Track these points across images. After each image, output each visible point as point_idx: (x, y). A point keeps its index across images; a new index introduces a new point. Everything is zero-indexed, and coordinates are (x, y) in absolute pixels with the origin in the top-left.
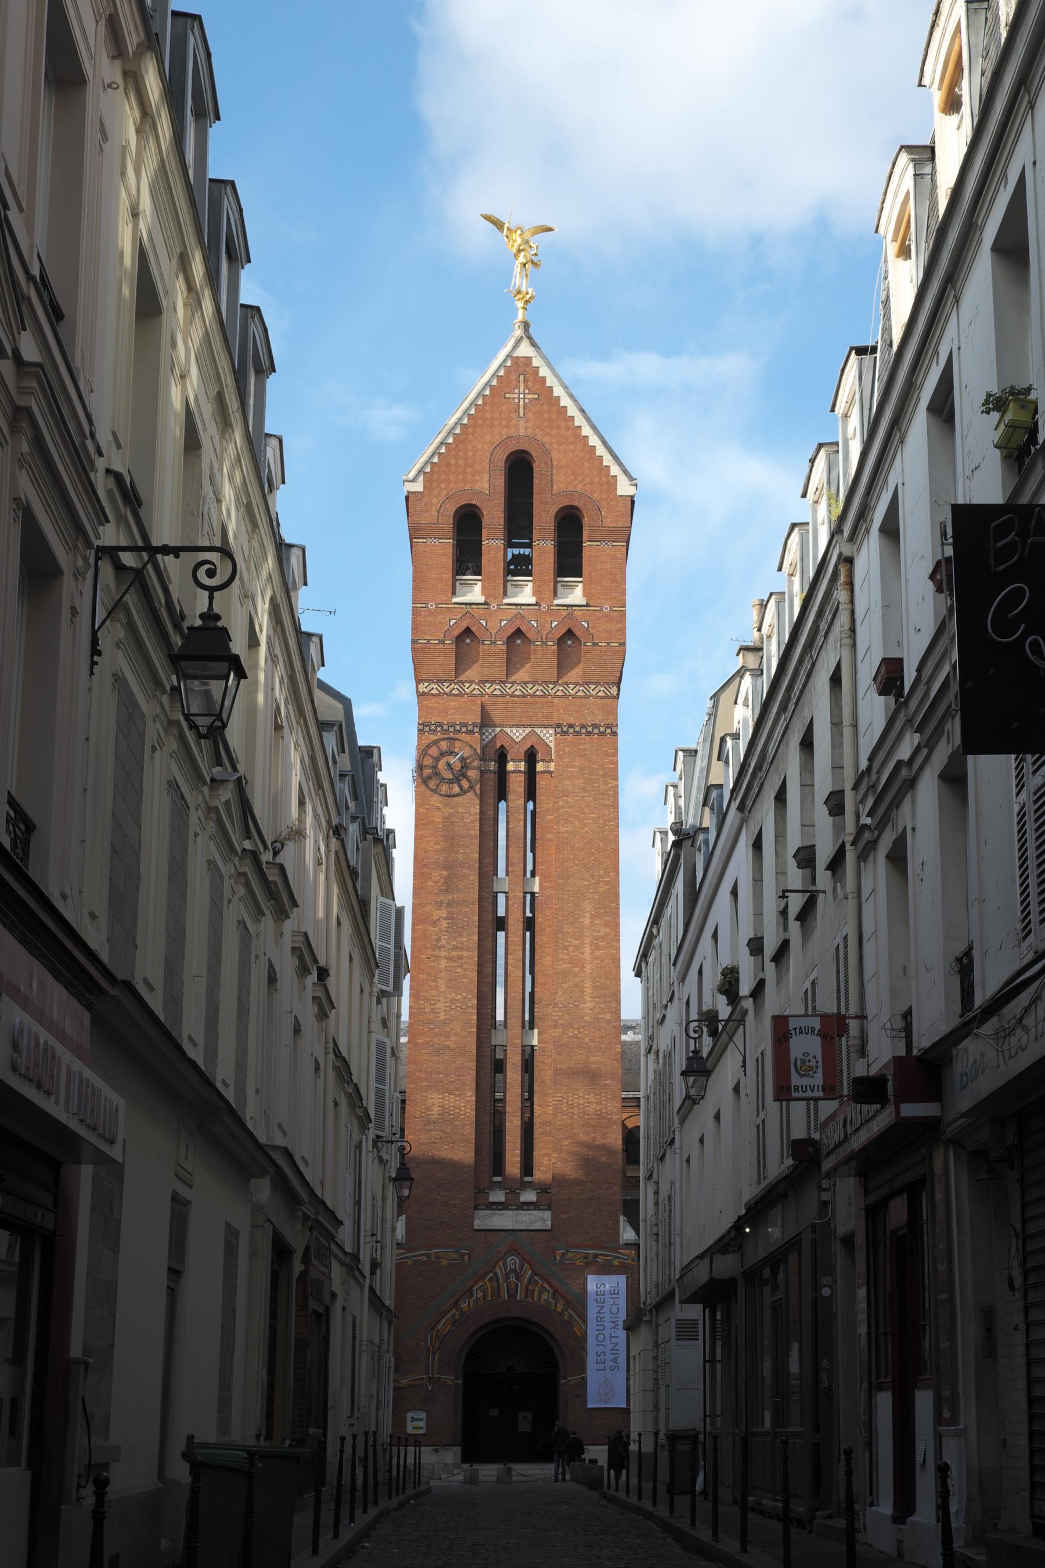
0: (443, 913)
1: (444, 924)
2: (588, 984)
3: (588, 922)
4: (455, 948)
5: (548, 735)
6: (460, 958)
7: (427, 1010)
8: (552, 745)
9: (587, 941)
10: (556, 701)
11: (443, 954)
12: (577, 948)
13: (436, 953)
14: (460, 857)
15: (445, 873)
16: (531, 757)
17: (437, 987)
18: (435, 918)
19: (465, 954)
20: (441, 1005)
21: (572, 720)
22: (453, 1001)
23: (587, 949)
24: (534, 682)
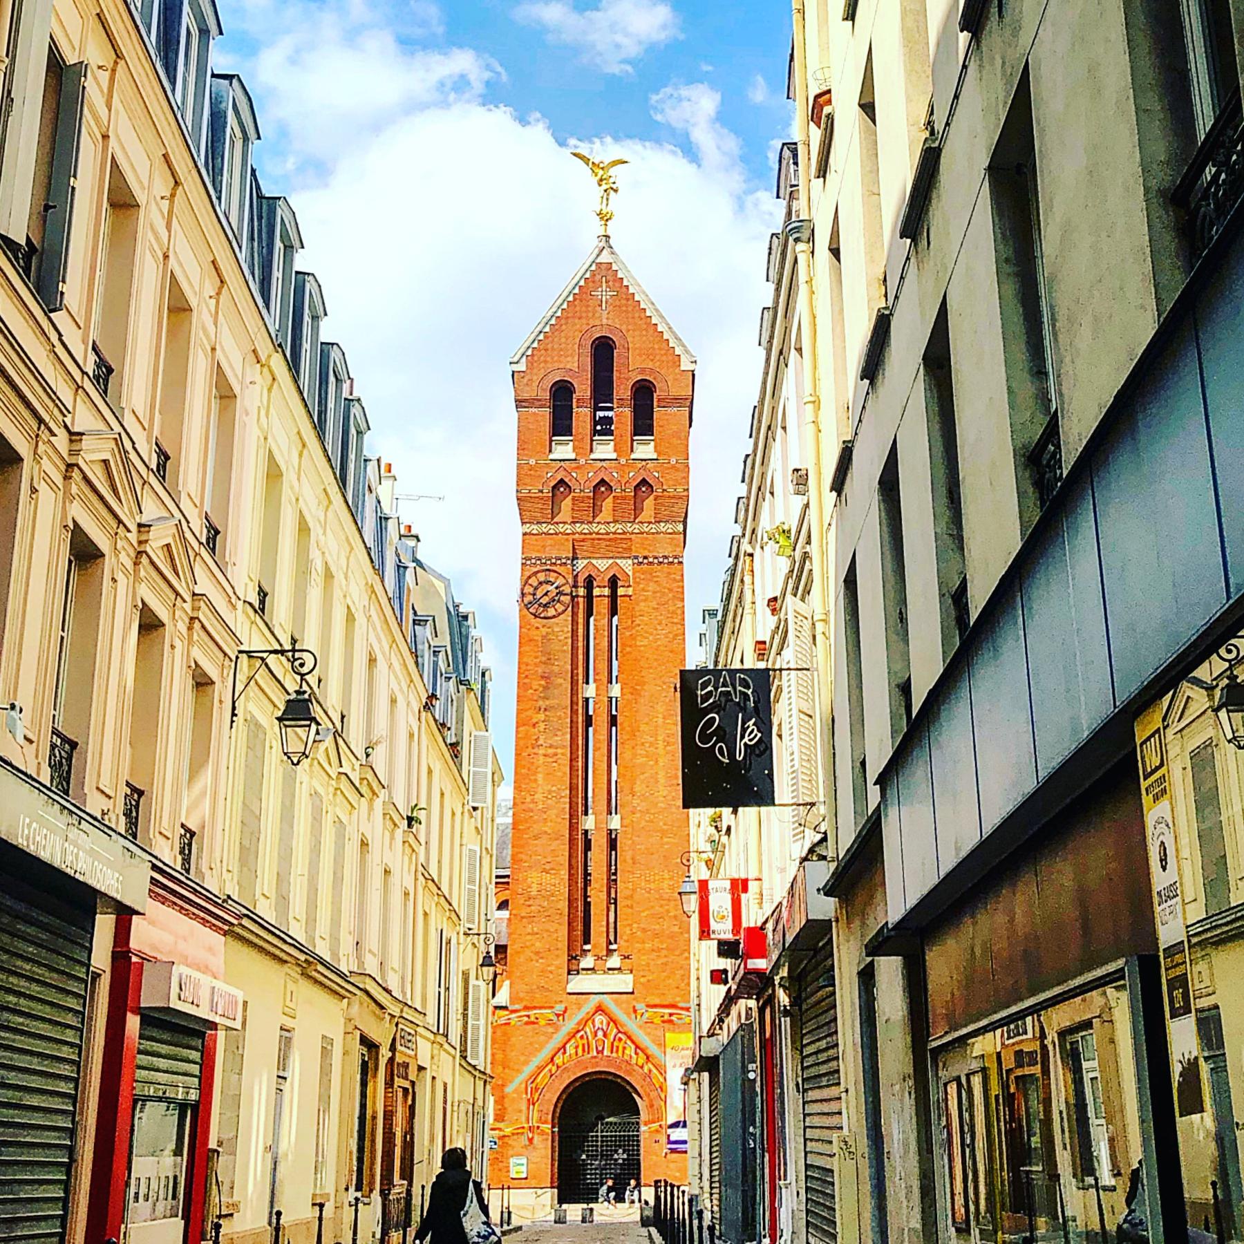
0: (542, 716)
1: (542, 726)
2: (661, 774)
3: (660, 720)
4: (551, 746)
5: (627, 565)
6: (556, 754)
7: (528, 800)
8: (630, 574)
9: (660, 738)
10: (633, 536)
11: (541, 751)
12: (651, 744)
13: (536, 750)
14: (556, 669)
15: (543, 682)
16: (613, 583)
17: (536, 780)
18: (534, 720)
19: (559, 751)
20: (538, 796)
21: (646, 553)
22: (550, 792)
23: (661, 744)
24: (615, 521)
